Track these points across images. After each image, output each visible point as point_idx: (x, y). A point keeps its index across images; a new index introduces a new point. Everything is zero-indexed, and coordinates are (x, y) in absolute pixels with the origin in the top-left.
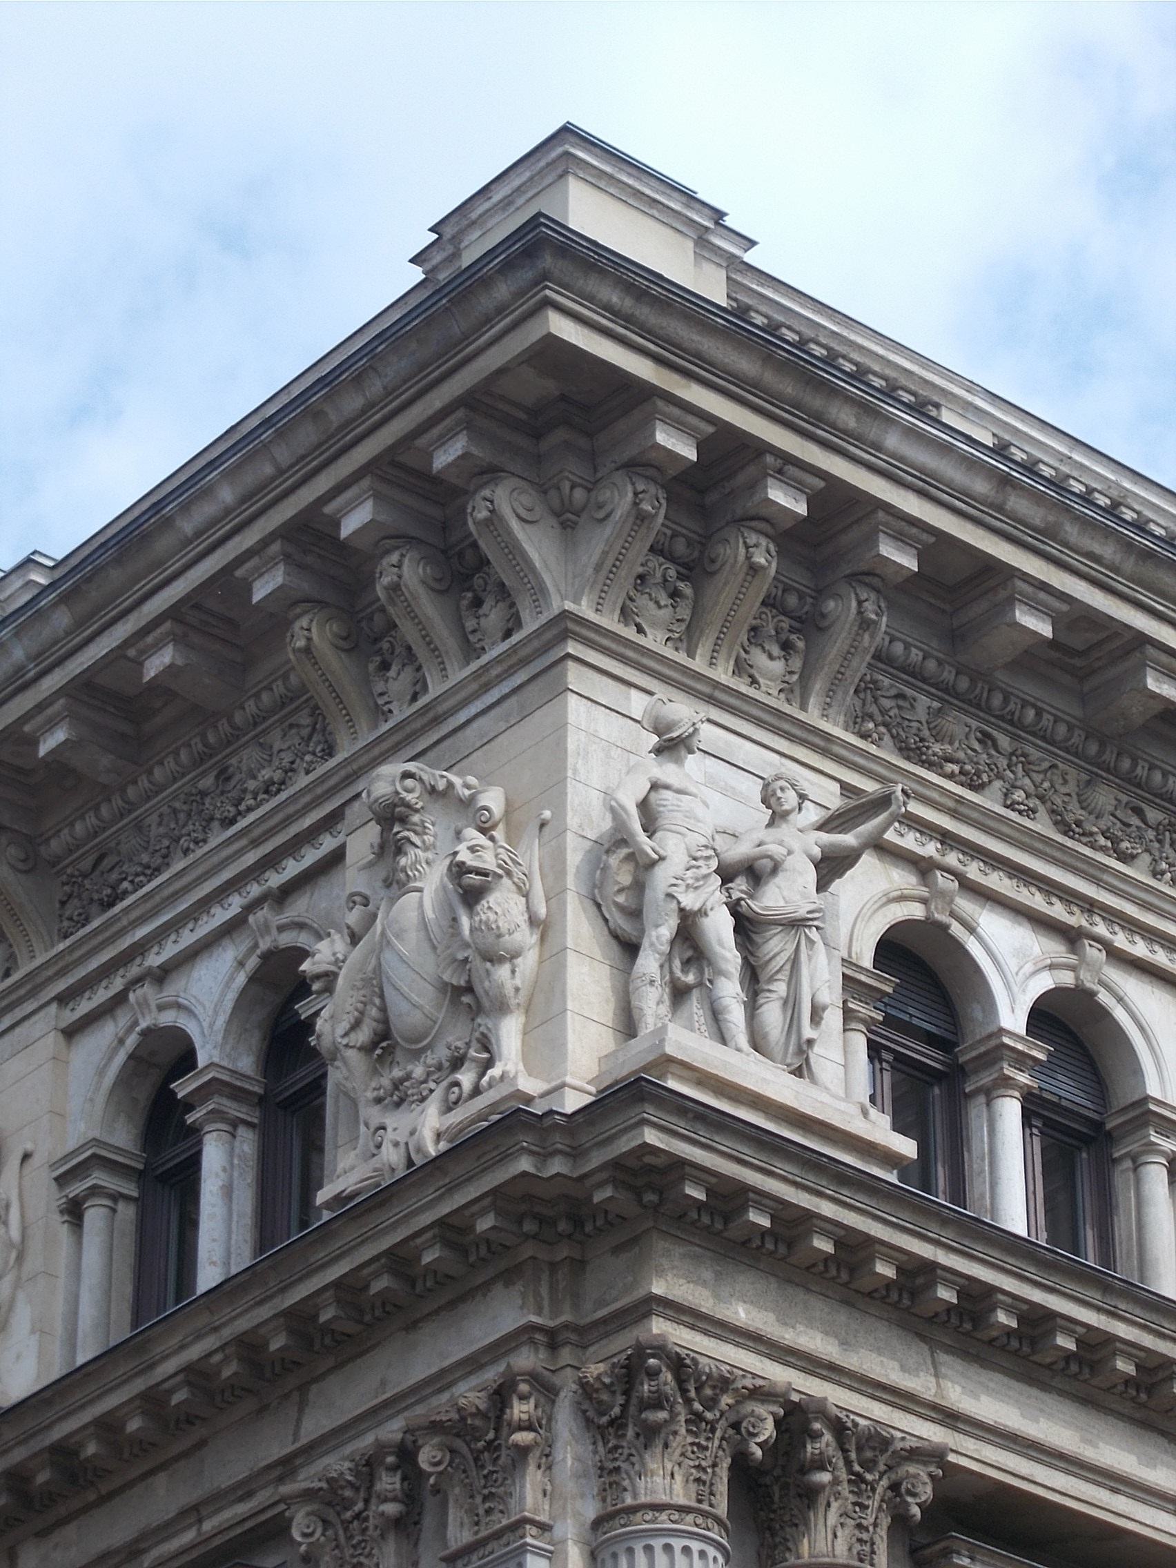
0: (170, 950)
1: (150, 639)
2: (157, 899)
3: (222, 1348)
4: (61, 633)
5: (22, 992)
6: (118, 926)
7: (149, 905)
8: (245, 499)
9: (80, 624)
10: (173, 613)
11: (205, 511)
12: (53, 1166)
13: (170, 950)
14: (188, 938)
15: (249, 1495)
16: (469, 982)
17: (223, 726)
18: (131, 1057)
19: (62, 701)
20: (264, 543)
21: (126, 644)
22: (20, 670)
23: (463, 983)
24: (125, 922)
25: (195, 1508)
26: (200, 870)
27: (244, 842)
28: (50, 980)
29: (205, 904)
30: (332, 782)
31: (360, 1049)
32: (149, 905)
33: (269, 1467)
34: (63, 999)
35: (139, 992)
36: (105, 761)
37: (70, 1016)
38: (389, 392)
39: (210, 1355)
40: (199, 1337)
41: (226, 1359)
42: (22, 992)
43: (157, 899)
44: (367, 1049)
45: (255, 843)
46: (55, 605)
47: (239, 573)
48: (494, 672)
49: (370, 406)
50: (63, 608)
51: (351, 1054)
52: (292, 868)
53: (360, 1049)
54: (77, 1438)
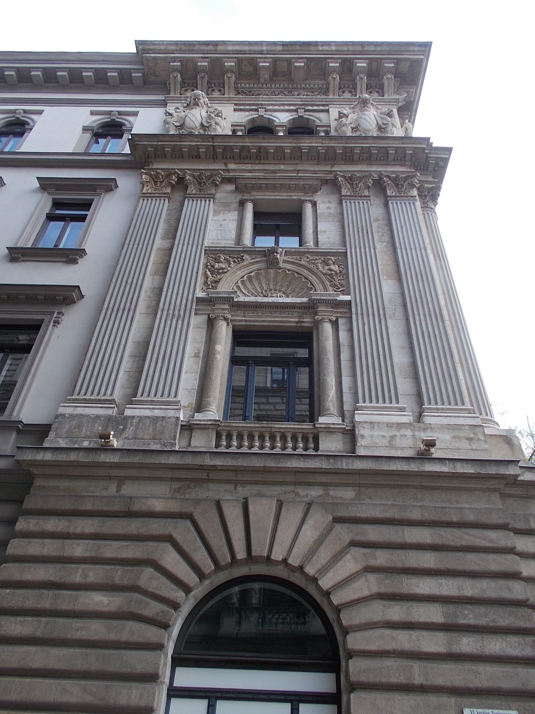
0: (271, 107)
1: (300, 60)
2: (272, 99)
3: (323, 147)
4: (278, 50)
5: (225, 99)
6: (259, 99)
7: (269, 99)
8: (336, 51)
9: (282, 51)
10: (307, 59)
11: (327, 48)
12: (232, 122)
13: (271, 107)
14: (276, 107)
15: (316, 174)
16: (385, 127)
17: (295, 86)
18: (253, 118)
19: (271, 60)
20: (338, 58)
21: (294, 58)
22: (263, 51)
23: (384, 127)
24: (261, 99)
25: (299, 171)
26: (286, 99)
27: (300, 100)
28: (234, 100)
29: (283, 105)
30: (327, 100)
31: (351, 127)
32: (269, 99)
33: (325, 171)
34: (235, 104)
35: (262, 109)
36: (267, 76)
37: (236, 107)
38: (380, 51)
39: (319, 147)
40: (317, 143)
41: (323, 149)
42: (225, 99)
43: (272, 99)
44: (353, 129)
45: (302, 101)
46: (280, 45)
47: (328, 60)
48: (376, 100)
49: (375, 51)
50: (281, 46)
51: (349, 127)
52: (310, 108)
53: (351, 127)
54: (269, 148)
